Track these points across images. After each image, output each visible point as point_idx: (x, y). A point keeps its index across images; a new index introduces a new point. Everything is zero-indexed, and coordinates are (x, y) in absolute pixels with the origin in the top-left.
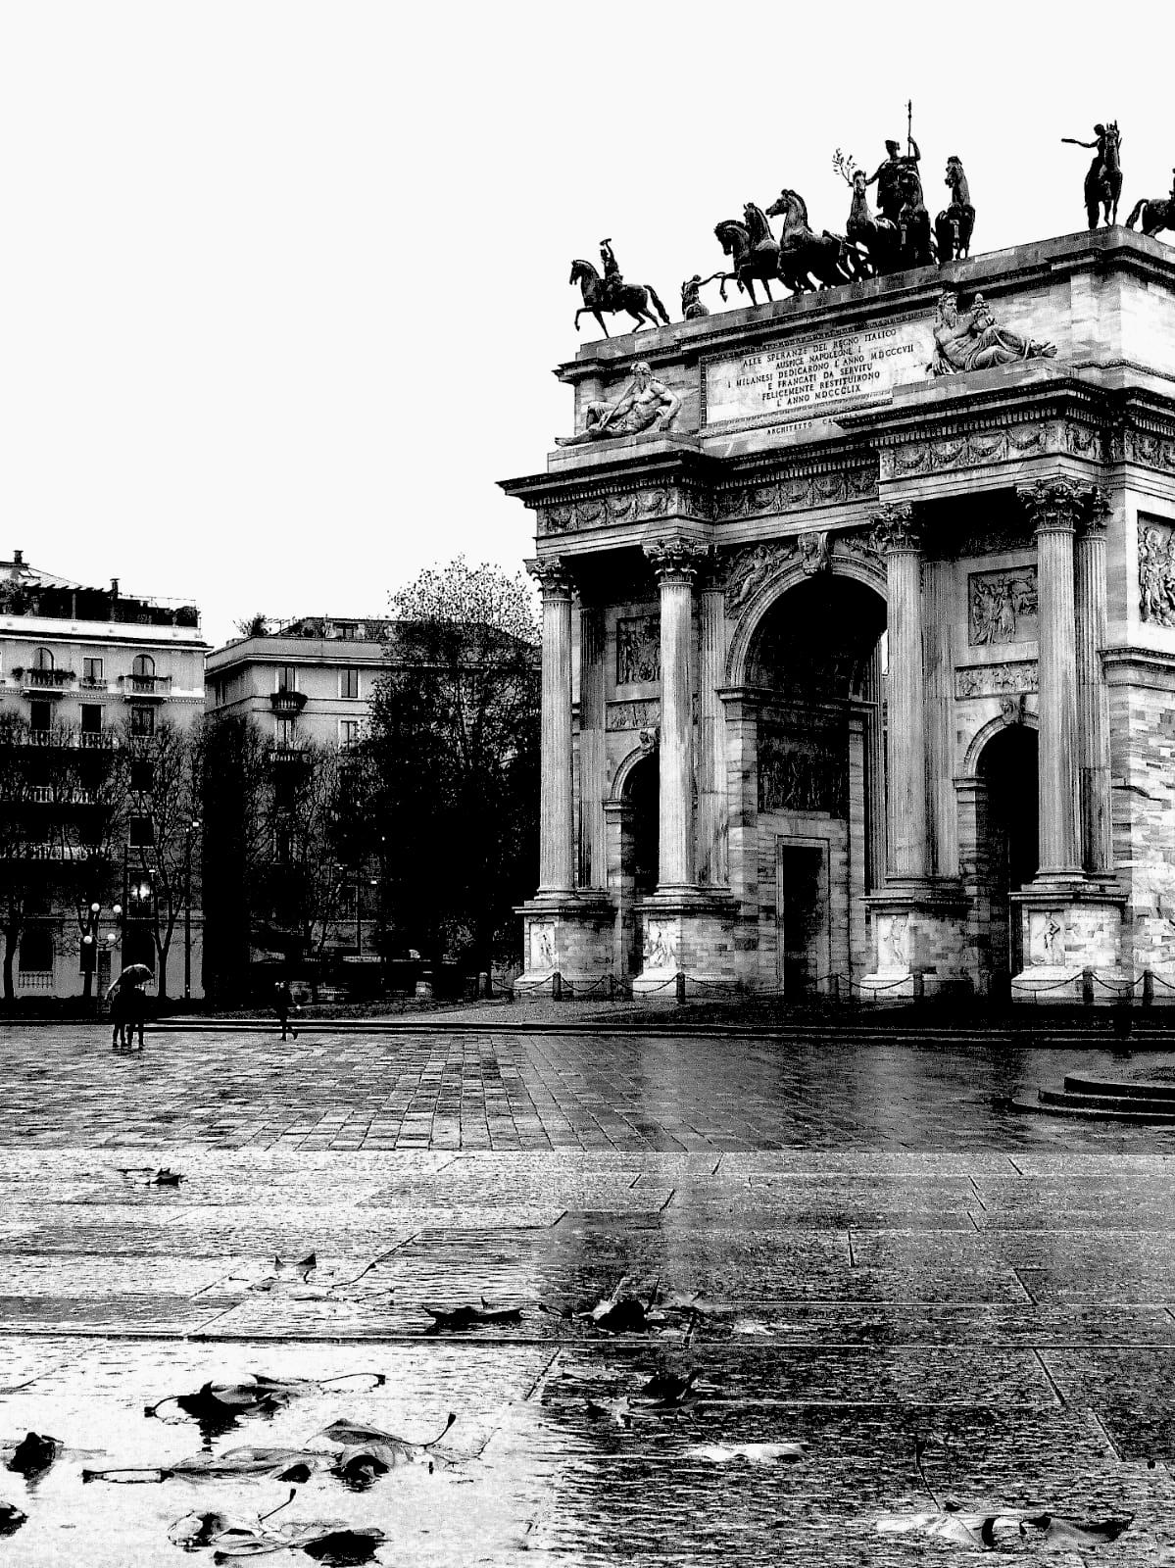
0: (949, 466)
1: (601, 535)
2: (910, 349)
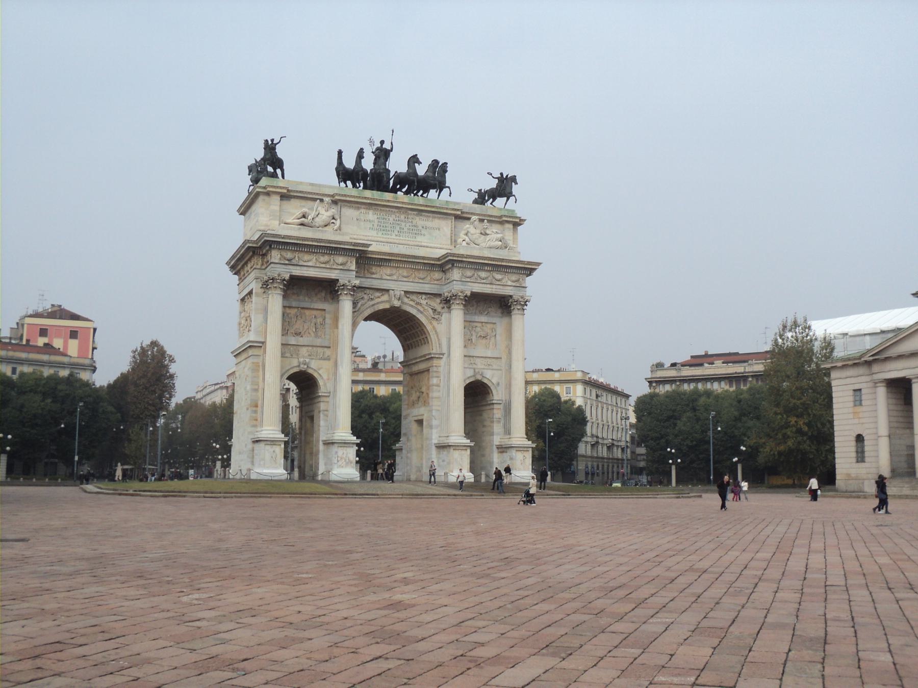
1: (311, 269)
2: (439, 229)
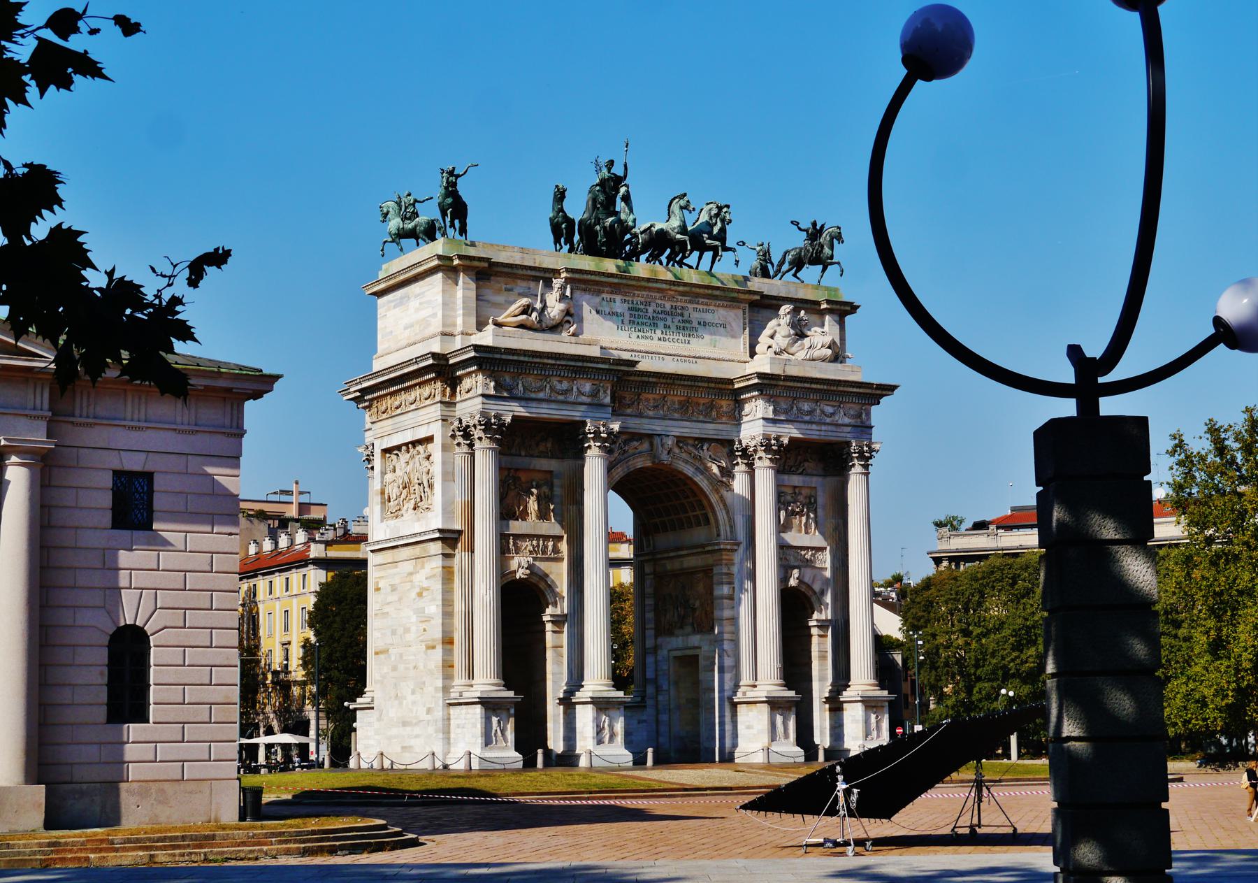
0: (807, 418)
2: (725, 327)
